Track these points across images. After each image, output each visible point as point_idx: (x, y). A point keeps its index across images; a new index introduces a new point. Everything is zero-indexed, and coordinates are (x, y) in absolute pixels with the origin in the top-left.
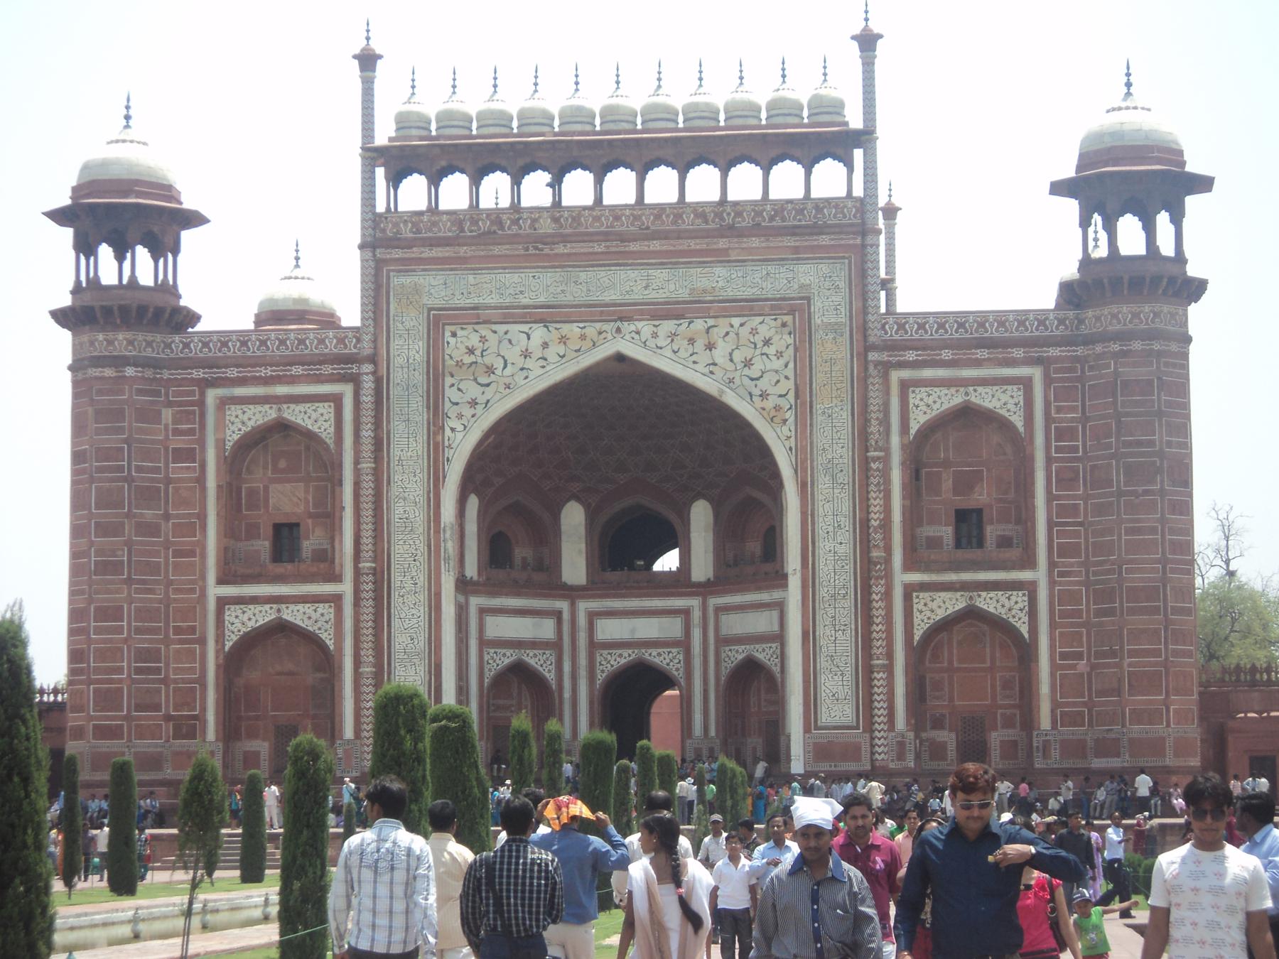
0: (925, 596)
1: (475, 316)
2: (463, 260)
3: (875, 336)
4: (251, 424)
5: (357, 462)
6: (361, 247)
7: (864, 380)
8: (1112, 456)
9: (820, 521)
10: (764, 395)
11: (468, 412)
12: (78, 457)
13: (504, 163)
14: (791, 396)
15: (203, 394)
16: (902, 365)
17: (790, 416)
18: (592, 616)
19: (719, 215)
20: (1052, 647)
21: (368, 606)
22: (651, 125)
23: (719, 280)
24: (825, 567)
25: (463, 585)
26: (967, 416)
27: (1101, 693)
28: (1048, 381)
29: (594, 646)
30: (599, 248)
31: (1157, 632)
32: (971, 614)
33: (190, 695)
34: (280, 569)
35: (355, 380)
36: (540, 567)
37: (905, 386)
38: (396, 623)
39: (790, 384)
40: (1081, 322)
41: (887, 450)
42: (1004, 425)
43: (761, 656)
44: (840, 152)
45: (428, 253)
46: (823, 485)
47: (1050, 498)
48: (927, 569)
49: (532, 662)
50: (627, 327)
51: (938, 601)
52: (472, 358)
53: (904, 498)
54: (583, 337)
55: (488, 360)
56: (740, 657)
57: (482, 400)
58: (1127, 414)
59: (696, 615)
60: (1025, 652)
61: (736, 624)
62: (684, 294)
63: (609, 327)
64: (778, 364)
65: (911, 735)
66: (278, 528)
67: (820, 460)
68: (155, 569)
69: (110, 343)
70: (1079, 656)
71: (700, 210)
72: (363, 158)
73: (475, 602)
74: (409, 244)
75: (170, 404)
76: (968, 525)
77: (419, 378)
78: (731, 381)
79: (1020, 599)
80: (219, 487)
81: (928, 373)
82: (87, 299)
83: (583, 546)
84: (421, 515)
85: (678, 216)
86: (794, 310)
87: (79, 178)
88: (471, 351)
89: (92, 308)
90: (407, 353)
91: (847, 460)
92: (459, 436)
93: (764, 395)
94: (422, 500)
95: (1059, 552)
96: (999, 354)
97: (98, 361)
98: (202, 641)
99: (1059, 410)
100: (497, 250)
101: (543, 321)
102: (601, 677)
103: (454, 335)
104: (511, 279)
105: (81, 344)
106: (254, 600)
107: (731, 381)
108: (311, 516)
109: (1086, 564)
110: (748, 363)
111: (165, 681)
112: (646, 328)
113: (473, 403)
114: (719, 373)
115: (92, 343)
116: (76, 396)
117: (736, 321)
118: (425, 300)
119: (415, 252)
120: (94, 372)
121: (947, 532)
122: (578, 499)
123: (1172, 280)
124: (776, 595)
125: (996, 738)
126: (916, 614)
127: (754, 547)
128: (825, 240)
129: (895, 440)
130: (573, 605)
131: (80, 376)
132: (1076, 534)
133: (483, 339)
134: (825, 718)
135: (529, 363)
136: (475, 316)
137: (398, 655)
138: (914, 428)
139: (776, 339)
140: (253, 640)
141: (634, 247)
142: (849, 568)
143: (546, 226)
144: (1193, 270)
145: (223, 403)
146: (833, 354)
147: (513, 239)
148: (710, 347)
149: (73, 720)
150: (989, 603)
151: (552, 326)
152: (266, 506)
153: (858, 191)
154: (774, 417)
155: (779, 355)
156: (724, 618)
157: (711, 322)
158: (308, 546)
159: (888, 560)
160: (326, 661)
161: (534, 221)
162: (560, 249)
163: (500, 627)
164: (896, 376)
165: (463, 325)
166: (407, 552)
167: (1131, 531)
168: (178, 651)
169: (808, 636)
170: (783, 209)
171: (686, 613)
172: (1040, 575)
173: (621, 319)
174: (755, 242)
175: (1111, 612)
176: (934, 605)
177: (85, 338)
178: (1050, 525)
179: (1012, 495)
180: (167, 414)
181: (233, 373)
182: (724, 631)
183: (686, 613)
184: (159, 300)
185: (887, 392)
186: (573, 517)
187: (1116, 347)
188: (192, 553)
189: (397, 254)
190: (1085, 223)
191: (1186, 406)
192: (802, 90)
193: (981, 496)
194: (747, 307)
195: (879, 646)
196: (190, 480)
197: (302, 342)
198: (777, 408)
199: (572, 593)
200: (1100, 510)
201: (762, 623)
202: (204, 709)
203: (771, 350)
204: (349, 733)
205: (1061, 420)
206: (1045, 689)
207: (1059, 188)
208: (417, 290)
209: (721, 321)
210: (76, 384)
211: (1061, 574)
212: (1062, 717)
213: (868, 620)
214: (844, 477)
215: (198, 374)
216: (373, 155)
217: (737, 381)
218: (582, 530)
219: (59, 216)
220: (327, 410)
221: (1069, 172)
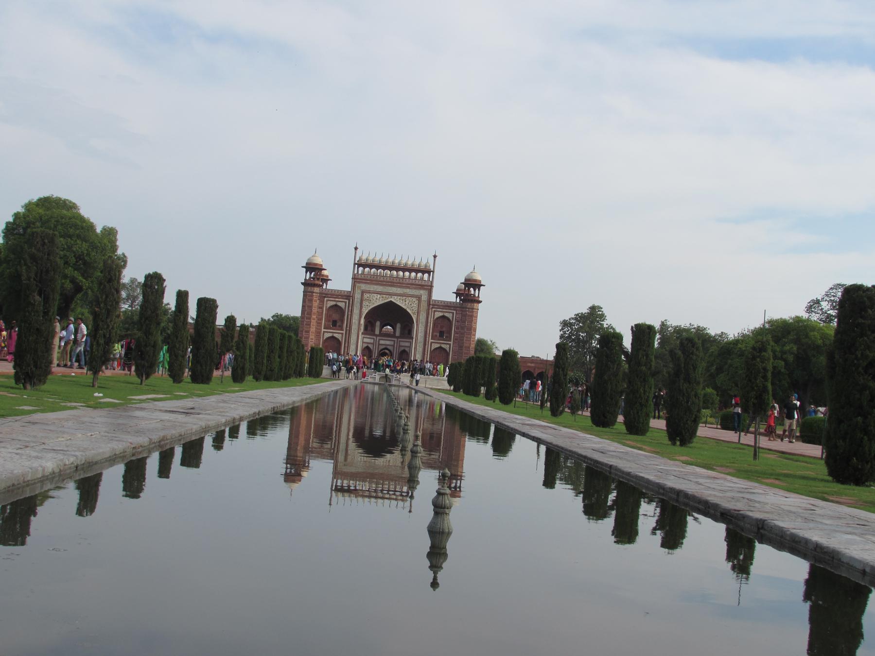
1: (369, 292)
7: (428, 309)
9: (419, 331)
23: (408, 291)
26: (443, 317)
42: (448, 319)
60: (448, 354)
61: (402, 344)
76: (442, 334)
86: (419, 298)
90: (358, 296)
95: (455, 339)
127: (407, 332)
136: (369, 292)
146: (424, 305)
150: (443, 346)
154: (414, 313)
160: (339, 343)
163: (366, 340)
172: (451, 343)
186: (378, 324)
193: (444, 329)
194: (412, 296)
199: (377, 336)
201: (407, 344)
216: (355, 264)
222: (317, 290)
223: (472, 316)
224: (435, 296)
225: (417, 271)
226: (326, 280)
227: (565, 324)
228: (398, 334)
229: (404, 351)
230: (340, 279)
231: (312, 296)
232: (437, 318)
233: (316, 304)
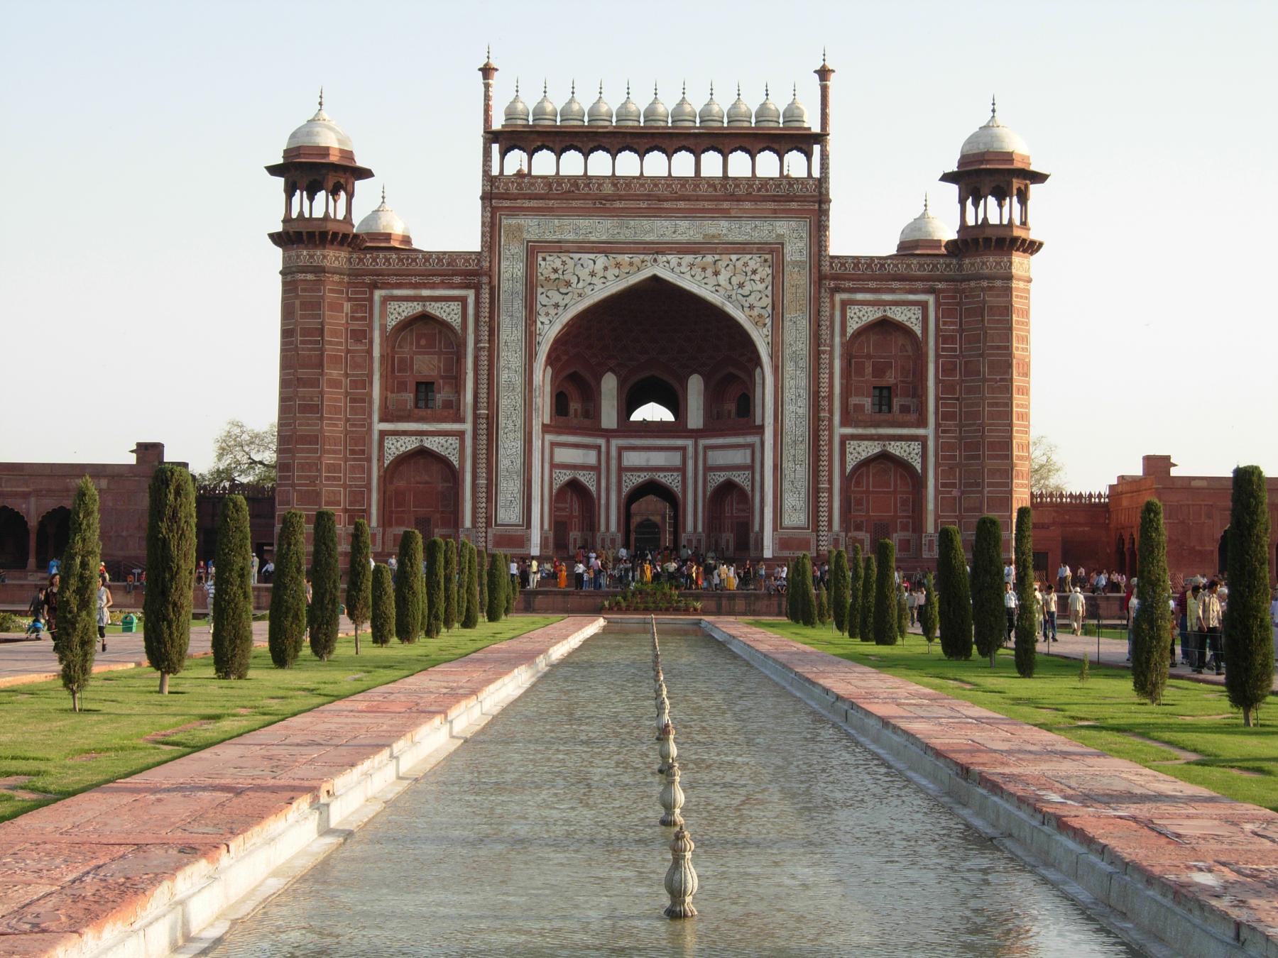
1: (559, 248)
2: (551, 209)
3: (826, 268)
4: (405, 314)
5: (477, 341)
6: (482, 198)
7: (818, 300)
8: (981, 355)
9: (783, 392)
10: (751, 307)
11: (552, 311)
12: (286, 334)
13: (579, 145)
14: (769, 309)
15: (372, 294)
17: (768, 321)
18: (621, 449)
19: (724, 186)
20: (936, 480)
21: (483, 439)
22: (680, 124)
23: (722, 228)
24: (789, 423)
26: (884, 325)
27: (967, 510)
30: (643, 205)
31: (1007, 471)
33: (359, 495)
34: (422, 413)
35: (477, 288)
36: (586, 414)
37: (844, 304)
38: (501, 451)
39: (769, 300)
40: (961, 266)
41: (832, 346)
43: (737, 480)
44: (804, 147)
45: (527, 204)
46: (789, 368)
47: (937, 381)
48: (856, 426)
49: (582, 479)
51: (863, 447)
52: (556, 276)
53: (842, 377)
54: (631, 264)
55: (566, 277)
56: (721, 480)
57: (562, 303)
58: (991, 328)
60: (917, 481)
61: (718, 458)
62: (699, 238)
63: (648, 258)
64: (761, 286)
65: (843, 534)
66: (418, 384)
67: (788, 351)
68: (337, 410)
69: (312, 257)
70: (954, 485)
71: (710, 181)
72: (485, 138)
73: (548, 437)
74: (515, 198)
75: (349, 299)
76: (884, 396)
77: (520, 287)
78: (730, 297)
79: (916, 447)
80: (382, 356)
81: (860, 296)
83: (615, 403)
84: (521, 378)
85: (697, 186)
86: (773, 251)
87: (289, 143)
88: (555, 271)
89: (299, 234)
90: (511, 269)
91: (805, 352)
92: (547, 327)
93: (751, 307)
94: (521, 370)
95: (943, 417)
96: (907, 285)
97: (304, 270)
98: (369, 460)
99: (945, 323)
101: (605, 252)
102: (625, 490)
103: (544, 259)
104: (584, 223)
105: (290, 257)
106: (405, 433)
107: (730, 297)
108: (442, 377)
109: (961, 426)
110: (741, 285)
111: (345, 486)
112: (673, 259)
113: (556, 306)
114: (722, 291)
115: (298, 257)
116: (285, 292)
117: (734, 257)
118: (525, 236)
119: (519, 203)
120: (301, 276)
121: (867, 402)
122: (614, 372)
123: (1024, 241)
124: (749, 439)
126: (848, 455)
127: (731, 407)
128: (794, 205)
129: (837, 339)
130: (608, 442)
131: (289, 278)
132: (954, 406)
133: (564, 263)
134: (786, 522)
135: (595, 280)
136: (559, 248)
137: (502, 473)
138: (850, 331)
139: (760, 270)
140: (404, 459)
142: (805, 423)
143: (608, 189)
146: (798, 281)
147: (584, 198)
148: (716, 273)
150: (896, 449)
151: (611, 256)
152: (412, 369)
153: (816, 173)
155: (762, 280)
156: (710, 453)
157: (717, 257)
158: (440, 397)
159: (831, 420)
160: (452, 474)
161: (600, 185)
162: (618, 204)
163: (564, 455)
164: (838, 297)
165: (550, 253)
166: (509, 403)
167: (991, 405)
168: (352, 466)
169: (778, 468)
170: (767, 184)
171: (684, 449)
172: (929, 431)
173: (657, 253)
174: (748, 205)
175: (977, 457)
176: (860, 450)
177: (294, 253)
178: (937, 399)
179: (910, 379)
181: (393, 280)
182: (710, 462)
183: (684, 449)
184: (343, 229)
185: (833, 307)
186: (609, 384)
187: (985, 284)
188: (363, 401)
189: (507, 203)
190: (962, 202)
191: (1027, 324)
192: (779, 104)
193: (890, 379)
194: (742, 248)
195: (824, 474)
196: (362, 351)
197: (440, 260)
198: (760, 316)
199: (608, 434)
200: (969, 390)
201: (740, 457)
202: (370, 505)
203: (757, 277)
204: (468, 524)
205: (946, 330)
206: (931, 506)
207: (947, 178)
208: (519, 228)
210: (285, 284)
211: (944, 431)
214: (801, 364)
215: (367, 280)
216: (492, 137)
217: (734, 297)
218: (615, 393)
219: (274, 170)
220: (456, 307)
221: (953, 167)
222: (334, 257)
223: (1007, 310)
228: (695, 419)
229: (729, 486)
231: (319, 283)
233: (337, 319)
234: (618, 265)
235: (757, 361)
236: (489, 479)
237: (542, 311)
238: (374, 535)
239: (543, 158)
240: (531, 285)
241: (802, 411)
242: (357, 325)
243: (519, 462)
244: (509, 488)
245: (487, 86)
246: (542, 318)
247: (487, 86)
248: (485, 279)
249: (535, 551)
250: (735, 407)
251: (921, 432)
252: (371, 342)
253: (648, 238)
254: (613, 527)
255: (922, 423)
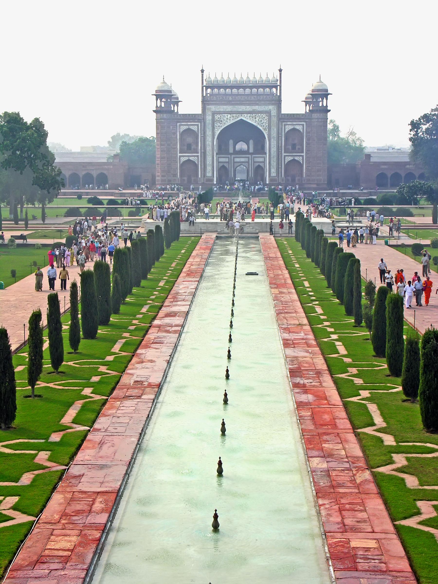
0: (287, 157)
3: (280, 117)
9: (271, 145)
11: (218, 128)
16: (284, 122)
18: (234, 158)
21: (202, 157)
23: (257, 108)
25: (217, 154)
26: (294, 130)
28: (306, 125)
29: (234, 162)
32: (294, 160)
38: (207, 160)
41: (282, 135)
45: (212, 103)
46: (272, 140)
50: (243, 115)
59: (250, 158)
60: (302, 165)
70: (309, 166)
77: (211, 122)
79: (301, 158)
81: (288, 123)
82: (159, 109)
86: (268, 113)
88: (219, 118)
90: (209, 118)
93: (263, 126)
97: (161, 119)
98: (177, 162)
100: (223, 102)
101: (230, 114)
102: (235, 167)
104: (225, 107)
110: (261, 121)
112: (246, 115)
113: (219, 126)
116: (157, 124)
119: (210, 102)
121: (290, 147)
124: (264, 156)
125: (297, 178)
128: (273, 102)
129: (283, 133)
134: (272, 175)
136: (219, 113)
137: (207, 165)
138: (286, 131)
140: (185, 162)
141: (244, 102)
144: (329, 109)
145: (180, 125)
146: (274, 120)
148: (255, 118)
149: (157, 174)
150: (296, 158)
153: (278, 94)
158: (192, 147)
159: (282, 152)
160: (196, 165)
162: (233, 102)
163: (221, 160)
164: (283, 123)
165: (217, 114)
166: (209, 149)
171: (248, 157)
174: (263, 102)
180: (171, 127)
186: (231, 142)
189: (207, 103)
192: (271, 78)
193: (296, 142)
199: (231, 154)
201: (261, 160)
204: (200, 177)
206: (304, 171)
208: (210, 108)
209: (257, 115)
212: (307, 175)
213: (278, 161)
214: (276, 139)
220: (196, 127)
224: (285, 110)
225: (264, 87)
226: (177, 103)
227: (415, 125)
228: (251, 150)
229: (259, 166)
230: (190, 104)
232: (288, 131)
234: (233, 117)
235: (265, 138)
236: (204, 166)
237: (216, 127)
238: (179, 179)
239: (216, 92)
240: (213, 121)
241: (275, 150)
242: (173, 131)
243: (211, 162)
244: (209, 168)
245: (203, 75)
246: (216, 129)
247: (203, 75)
248: (202, 120)
249: (215, 183)
250: (260, 148)
251: (302, 154)
252: (177, 135)
253: (240, 110)
254: (232, 176)
255: (303, 152)
